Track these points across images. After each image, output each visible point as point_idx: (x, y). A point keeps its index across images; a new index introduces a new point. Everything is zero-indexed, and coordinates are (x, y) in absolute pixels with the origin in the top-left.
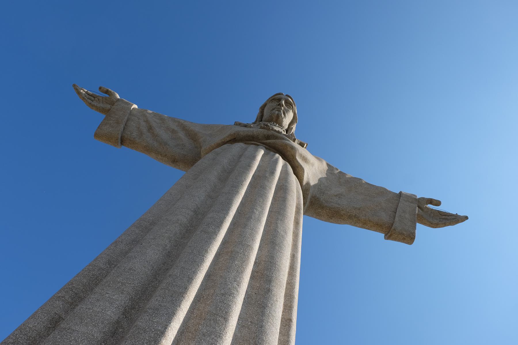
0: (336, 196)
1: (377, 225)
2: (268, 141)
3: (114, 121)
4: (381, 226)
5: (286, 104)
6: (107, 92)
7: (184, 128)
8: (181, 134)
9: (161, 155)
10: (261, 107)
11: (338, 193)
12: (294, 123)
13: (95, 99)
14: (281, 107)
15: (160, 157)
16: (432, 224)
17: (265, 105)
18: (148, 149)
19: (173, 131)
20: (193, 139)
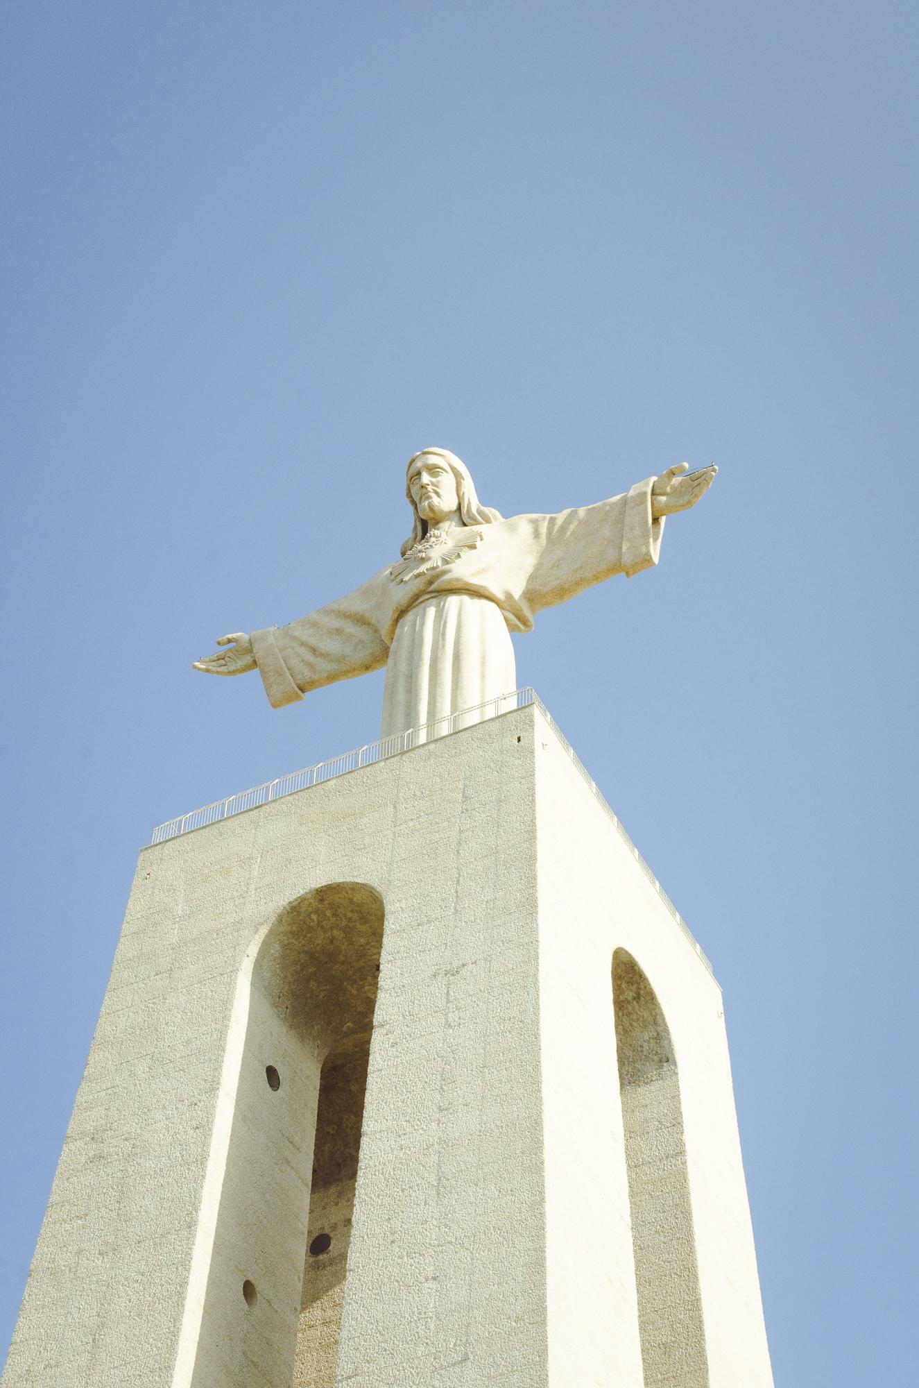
0: (552, 567)
1: (609, 570)
2: (432, 588)
3: (274, 675)
4: (613, 569)
5: (431, 472)
6: (229, 641)
7: (345, 616)
8: (350, 628)
9: (349, 672)
10: (407, 495)
11: (552, 562)
12: (461, 482)
13: (227, 659)
14: (426, 488)
15: (350, 675)
16: (684, 506)
17: (409, 490)
18: (332, 678)
19: (338, 631)
20: (365, 624)
